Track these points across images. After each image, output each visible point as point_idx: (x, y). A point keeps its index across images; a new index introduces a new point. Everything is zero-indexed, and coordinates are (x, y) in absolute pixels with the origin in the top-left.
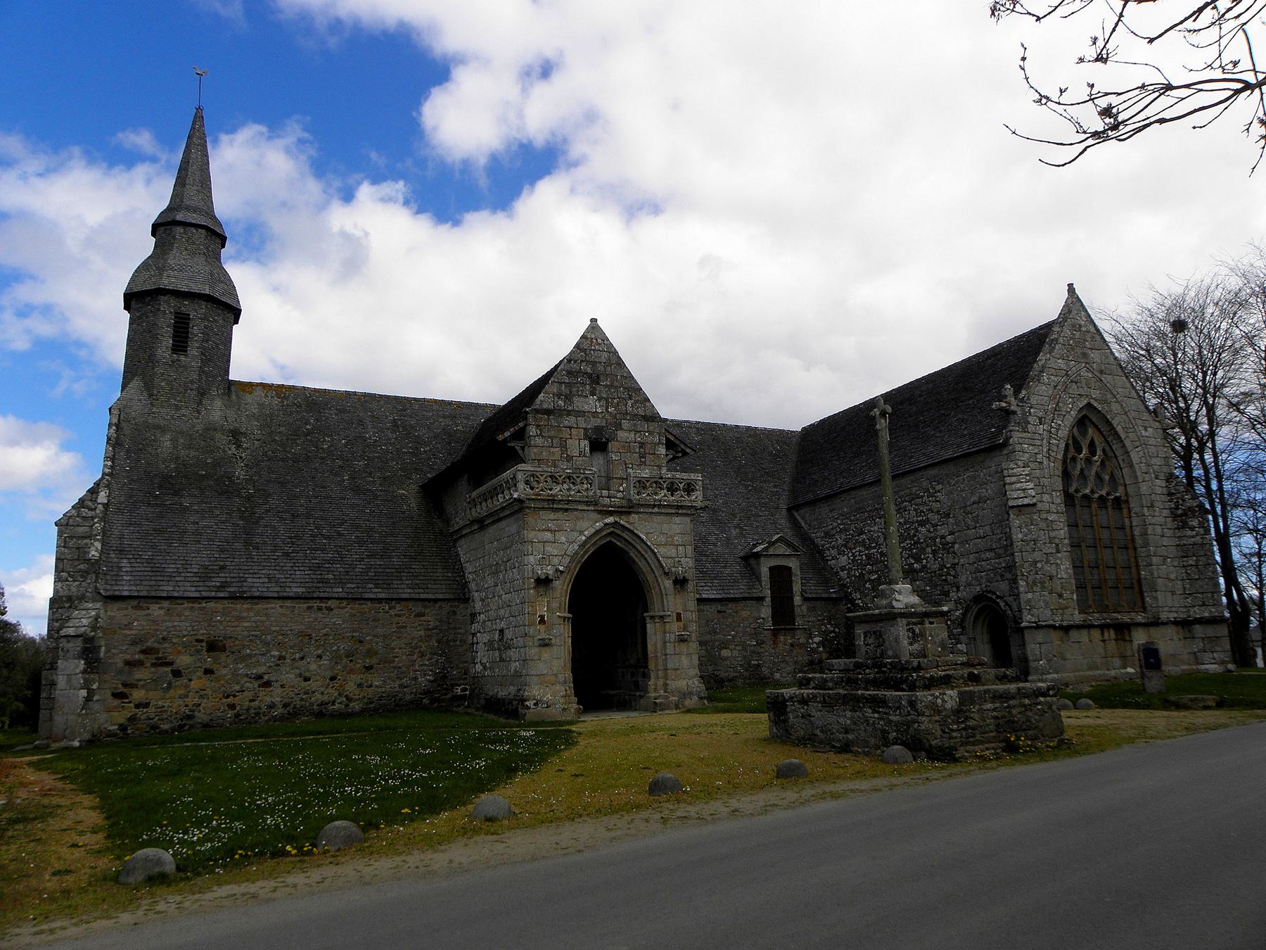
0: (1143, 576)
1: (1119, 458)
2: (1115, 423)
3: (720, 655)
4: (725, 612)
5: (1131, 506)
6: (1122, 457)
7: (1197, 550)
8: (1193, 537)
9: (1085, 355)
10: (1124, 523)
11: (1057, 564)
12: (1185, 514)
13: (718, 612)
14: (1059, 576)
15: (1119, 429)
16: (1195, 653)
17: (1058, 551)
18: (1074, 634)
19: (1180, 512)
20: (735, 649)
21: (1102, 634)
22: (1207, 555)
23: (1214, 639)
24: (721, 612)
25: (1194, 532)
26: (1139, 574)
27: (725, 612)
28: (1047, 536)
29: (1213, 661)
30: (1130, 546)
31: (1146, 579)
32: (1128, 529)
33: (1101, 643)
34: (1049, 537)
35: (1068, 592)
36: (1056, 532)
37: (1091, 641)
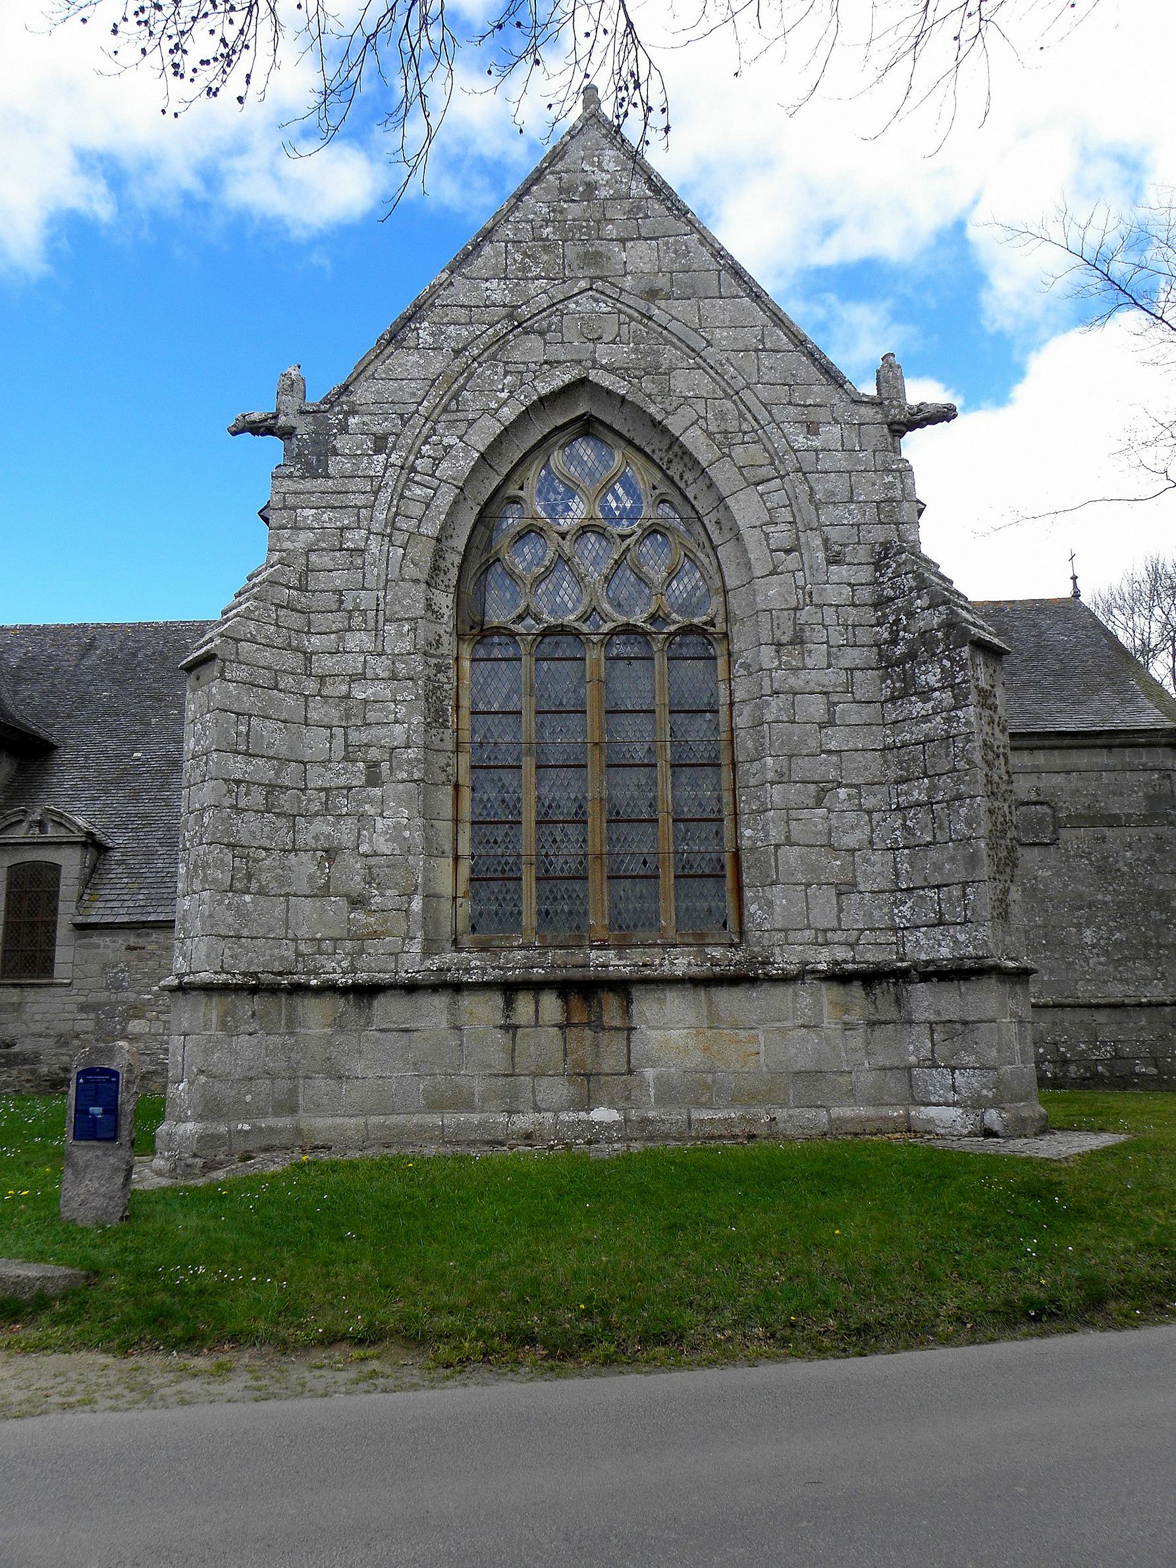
0: (745, 843)
1: (706, 520)
2: (674, 425)
3: (124, 1029)
4: (143, 948)
5: (736, 648)
6: (713, 516)
7: (933, 755)
8: (926, 718)
9: (593, 258)
10: (714, 695)
11: (361, 816)
12: (912, 656)
13: (129, 948)
14: (364, 848)
15: (695, 440)
16: (909, 1068)
17: (373, 779)
18: (388, 1008)
19: (900, 649)
20: (158, 1019)
21: (509, 1004)
22: (955, 770)
23: (958, 1026)
24: (135, 948)
25: (931, 704)
26: (737, 836)
27: (143, 948)
28: (339, 741)
29: (952, 1097)
30: (725, 759)
31: (753, 849)
32: (724, 710)
33: (499, 1034)
34: (347, 746)
35: (388, 892)
36: (375, 731)
37: (458, 1028)
